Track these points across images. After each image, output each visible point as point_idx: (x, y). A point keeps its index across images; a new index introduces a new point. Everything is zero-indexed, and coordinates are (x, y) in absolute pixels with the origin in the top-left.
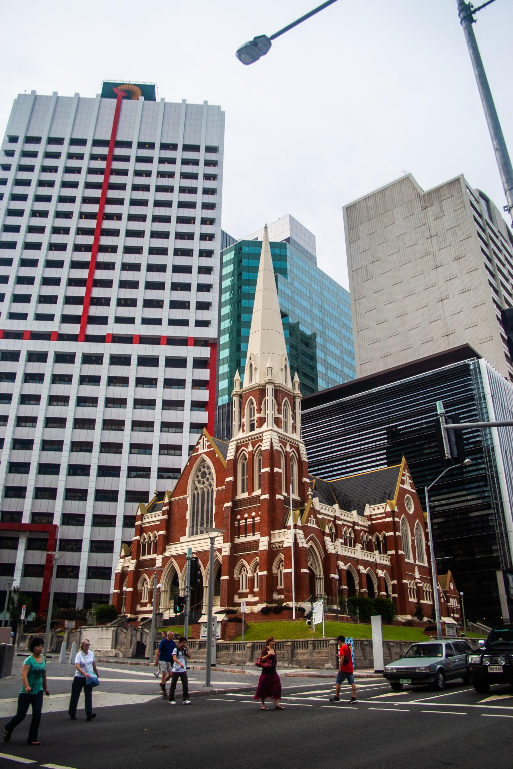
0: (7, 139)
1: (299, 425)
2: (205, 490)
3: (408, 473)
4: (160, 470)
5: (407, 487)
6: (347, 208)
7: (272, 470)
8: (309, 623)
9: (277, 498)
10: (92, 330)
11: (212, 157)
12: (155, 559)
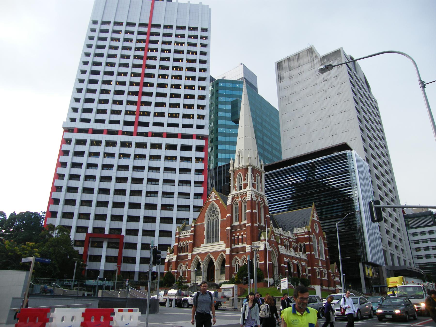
0: (91, 22)
1: (264, 187)
2: (214, 220)
3: (316, 211)
4: (179, 206)
5: (315, 219)
6: (277, 63)
7: (252, 211)
8: (279, 289)
9: (255, 225)
10: (141, 129)
11: (204, 34)
12: (187, 255)
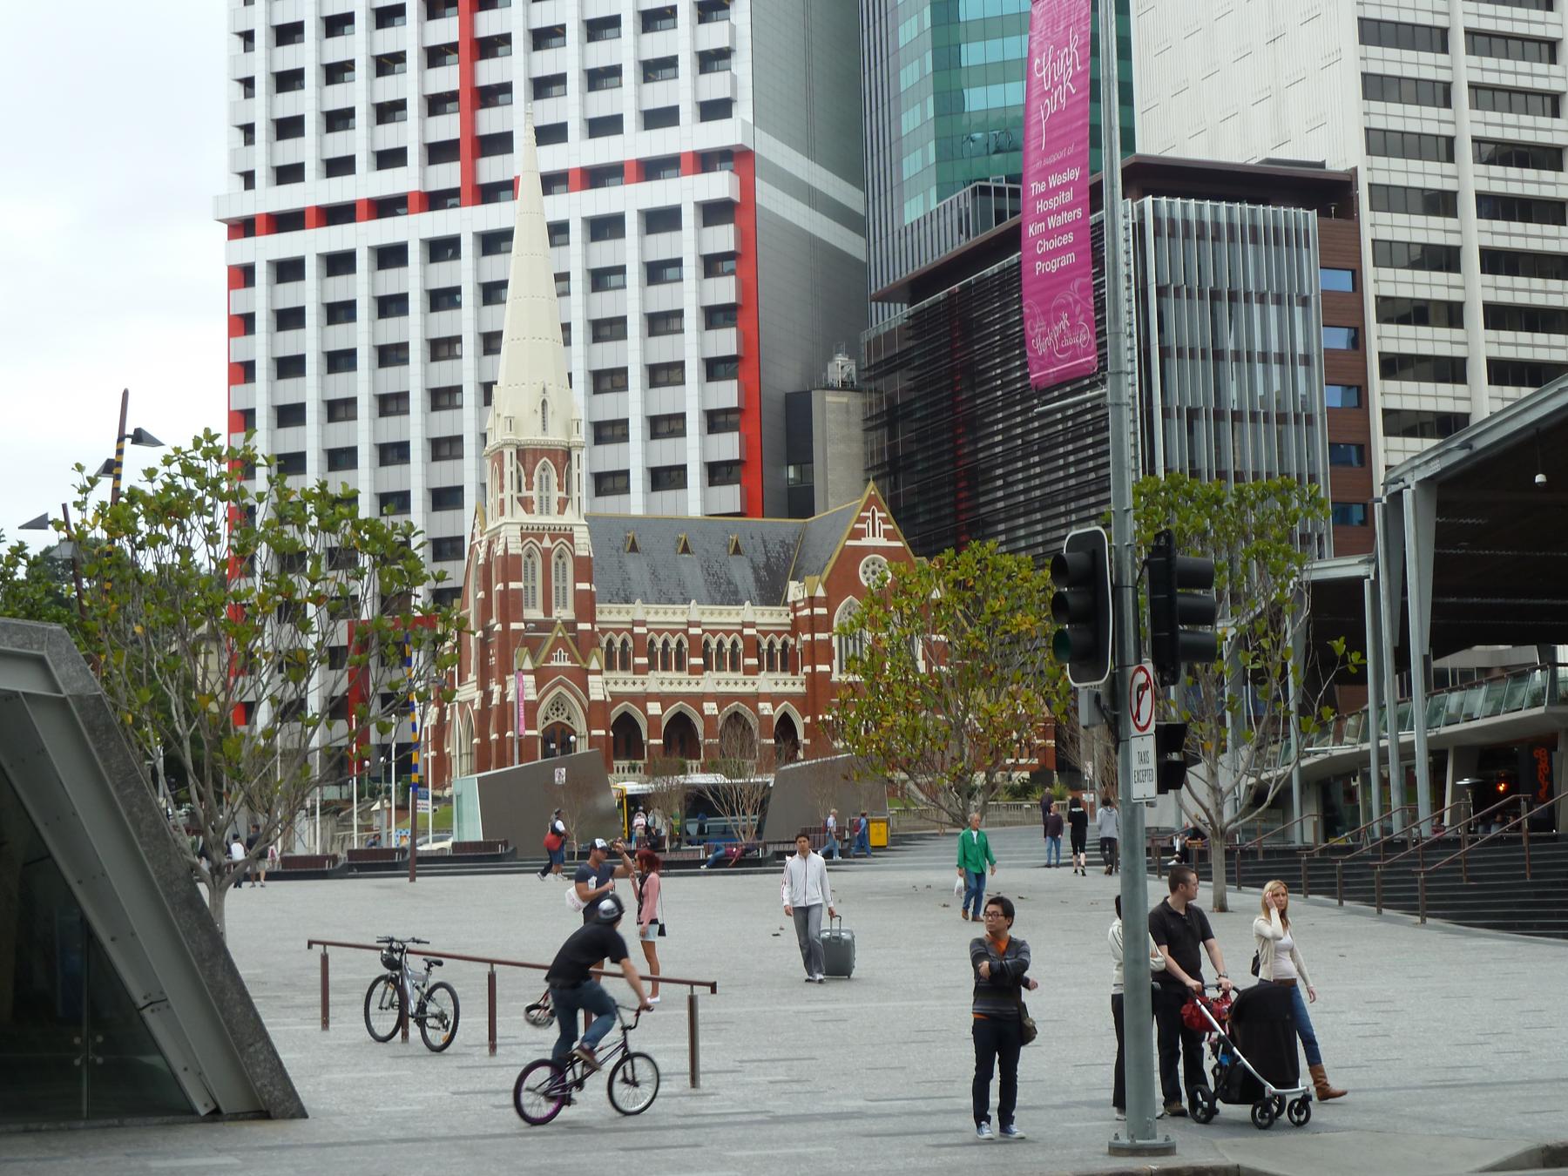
7: (506, 586)
